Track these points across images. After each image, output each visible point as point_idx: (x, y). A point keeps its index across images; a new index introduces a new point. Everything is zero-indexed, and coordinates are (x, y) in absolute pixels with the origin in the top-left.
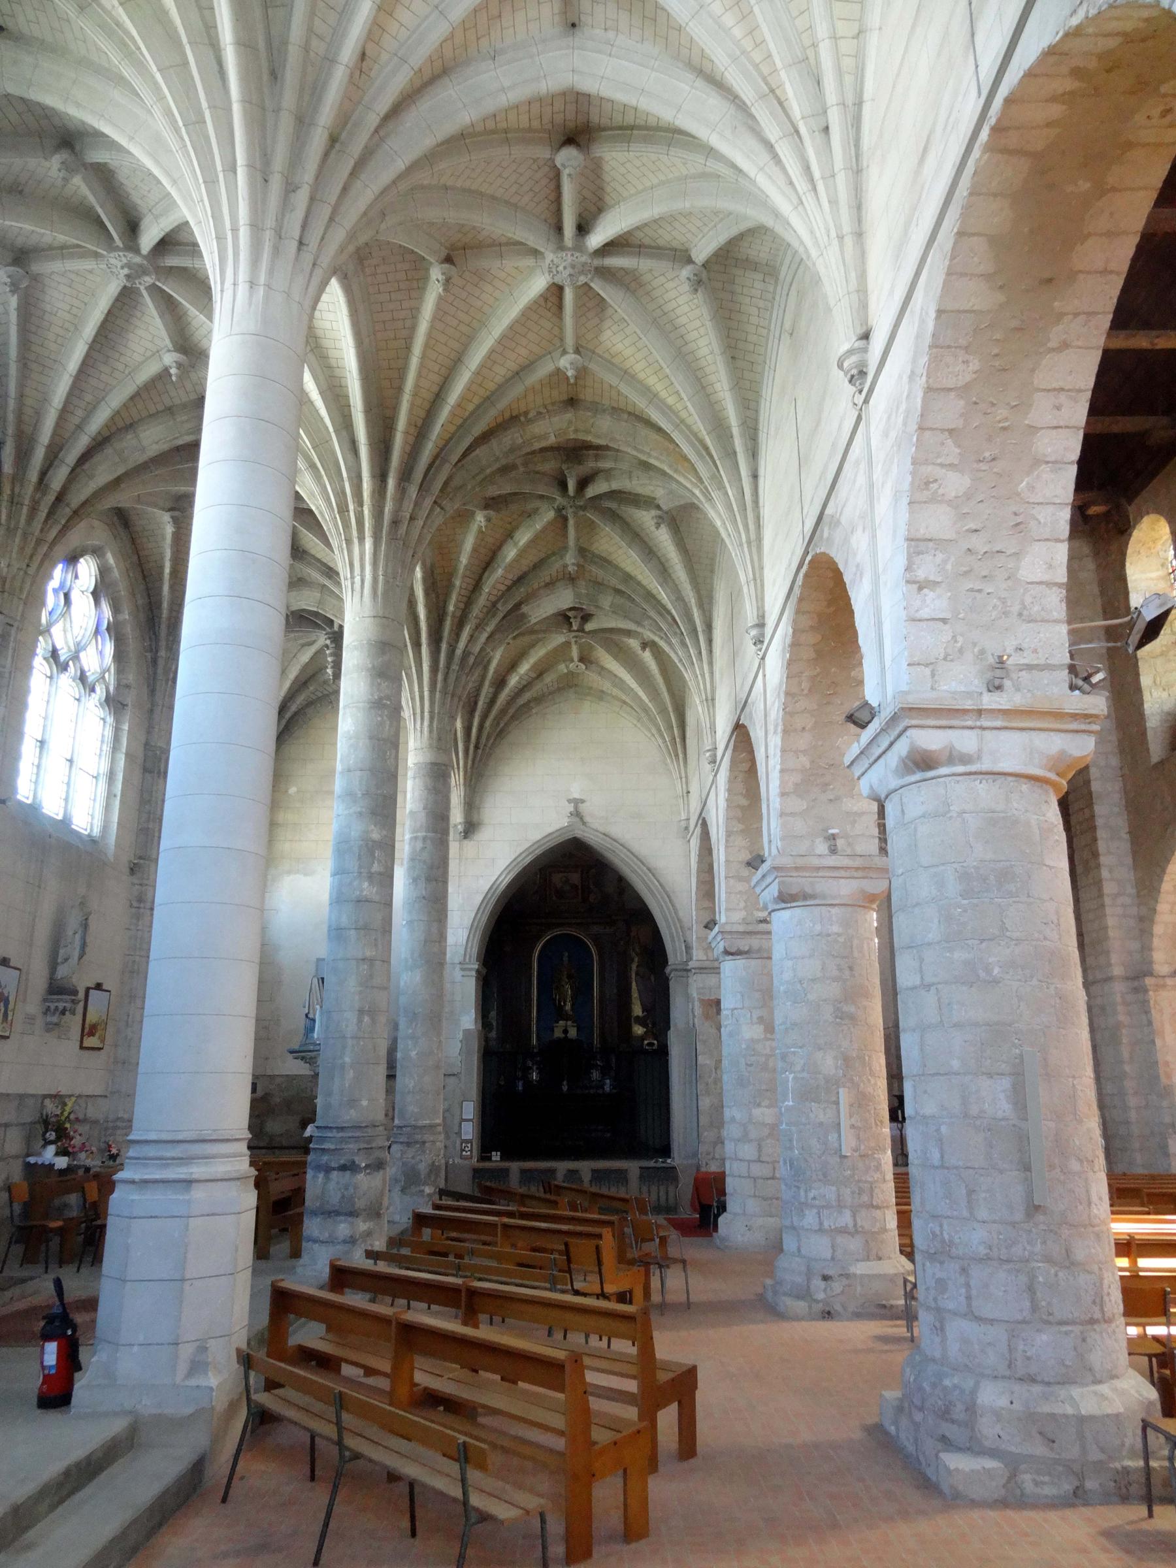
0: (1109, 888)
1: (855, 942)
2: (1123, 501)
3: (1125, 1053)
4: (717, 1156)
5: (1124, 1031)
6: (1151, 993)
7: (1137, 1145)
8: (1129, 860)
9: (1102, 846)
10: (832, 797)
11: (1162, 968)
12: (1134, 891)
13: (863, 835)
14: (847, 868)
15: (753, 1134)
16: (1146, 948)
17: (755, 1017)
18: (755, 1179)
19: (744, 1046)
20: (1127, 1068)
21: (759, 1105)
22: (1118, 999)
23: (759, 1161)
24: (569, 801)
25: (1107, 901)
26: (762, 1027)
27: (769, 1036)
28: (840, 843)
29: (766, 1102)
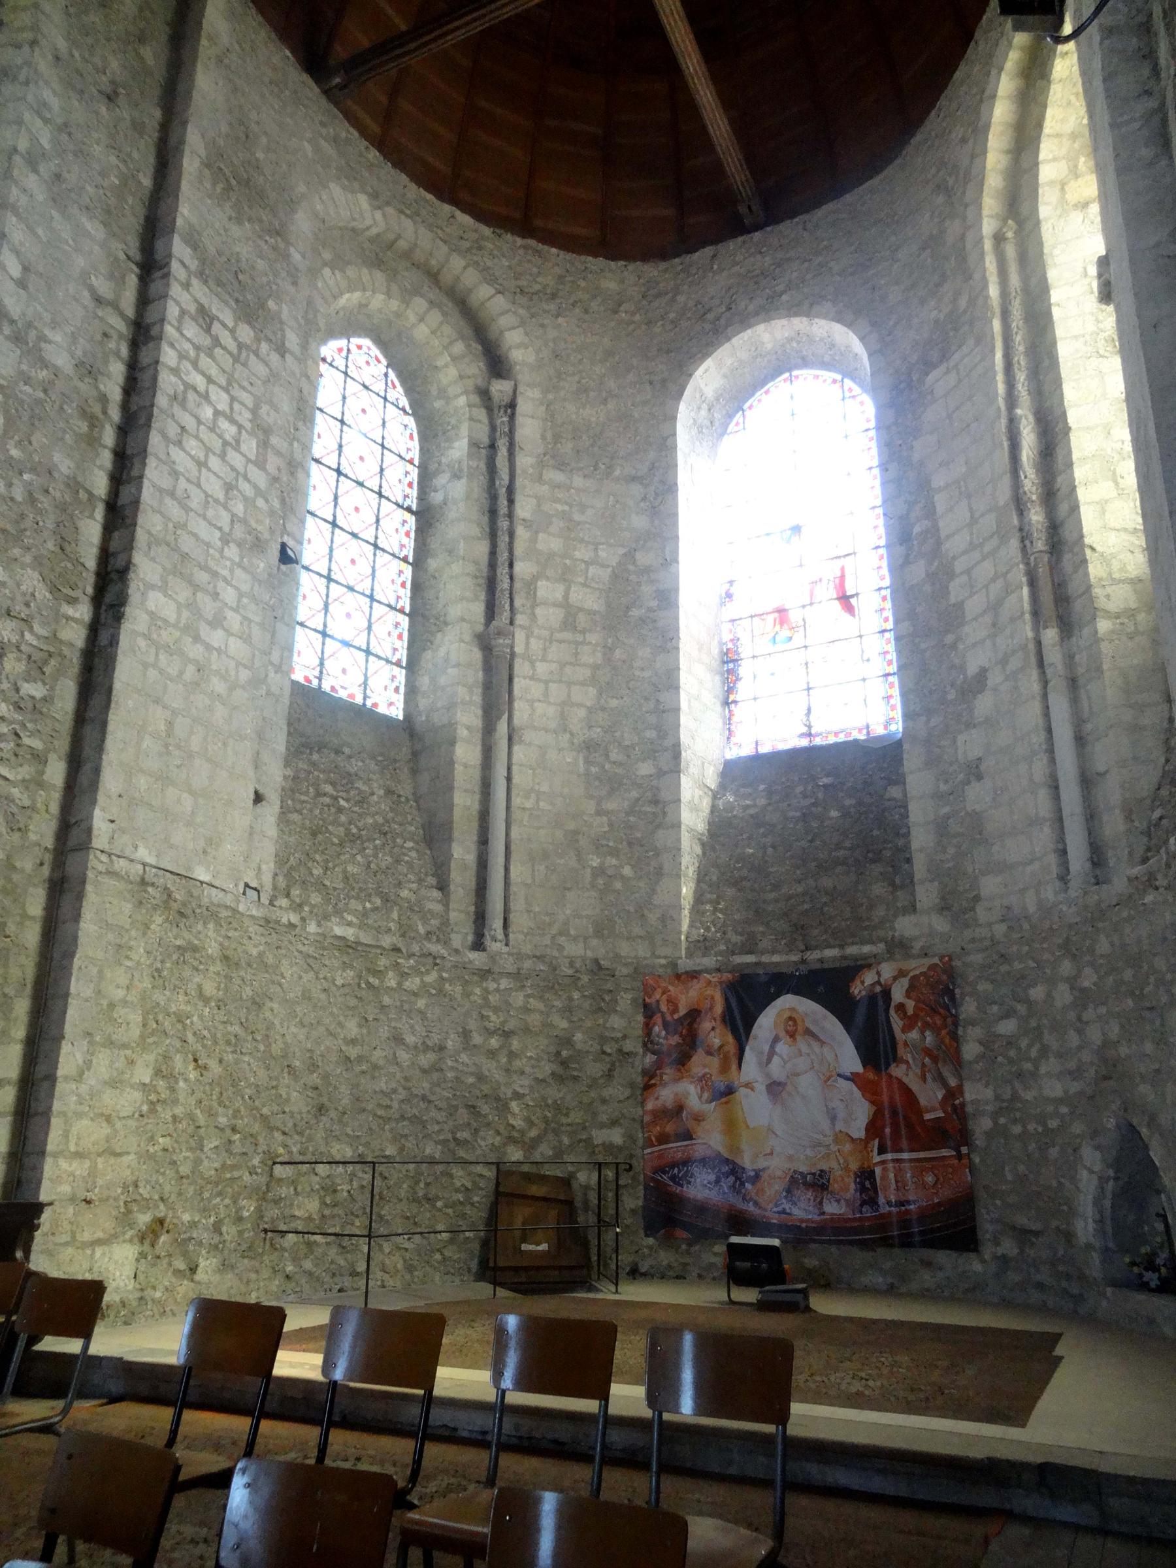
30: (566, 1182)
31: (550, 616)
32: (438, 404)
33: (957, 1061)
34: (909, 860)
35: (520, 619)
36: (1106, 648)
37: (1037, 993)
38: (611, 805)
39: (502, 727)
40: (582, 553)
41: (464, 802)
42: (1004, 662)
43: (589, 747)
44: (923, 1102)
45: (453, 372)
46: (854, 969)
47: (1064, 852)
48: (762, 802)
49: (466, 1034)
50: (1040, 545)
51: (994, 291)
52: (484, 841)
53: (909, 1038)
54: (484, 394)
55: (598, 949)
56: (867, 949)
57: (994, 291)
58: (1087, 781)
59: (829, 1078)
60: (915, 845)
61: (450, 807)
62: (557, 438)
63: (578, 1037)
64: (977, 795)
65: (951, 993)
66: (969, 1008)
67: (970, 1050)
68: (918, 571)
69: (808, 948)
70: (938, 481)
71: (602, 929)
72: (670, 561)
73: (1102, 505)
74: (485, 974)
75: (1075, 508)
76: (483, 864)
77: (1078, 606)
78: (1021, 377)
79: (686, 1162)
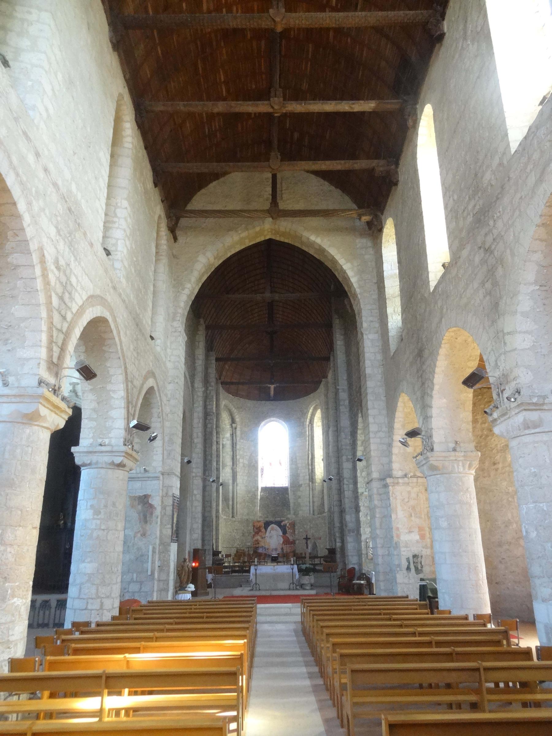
0: (373, 428)
1: (8, 448)
2: (379, 214)
3: (378, 524)
4: (130, 590)
5: (377, 510)
6: (390, 487)
7: (381, 578)
8: (384, 412)
9: (370, 404)
10: (10, 348)
11: (397, 472)
12: (387, 429)
13: (28, 373)
14: (8, 396)
15: (78, 581)
16: (390, 462)
17: (89, 504)
18: (75, 610)
19: (81, 524)
20: (378, 532)
21: (83, 562)
22: (375, 491)
23: (79, 598)
24: (70, 384)
25: (371, 435)
26: (92, 511)
27: (96, 517)
28: (11, 379)
29: (89, 560)
30: (244, 550)
31: (241, 465)
32: (224, 426)
33: (294, 534)
34: (290, 507)
35: (238, 466)
36: (317, 487)
37: (305, 526)
38: (249, 495)
39: (235, 484)
40: (245, 454)
41: (231, 495)
42: (305, 484)
43: (246, 486)
44: (290, 539)
45: (228, 422)
46: (282, 521)
47: (310, 511)
48: (268, 495)
49: (233, 530)
50: (310, 471)
51: (307, 433)
52: (233, 501)
53: (289, 531)
54: (231, 425)
55: (247, 517)
56: (284, 519)
57: (307, 433)
58: (313, 502)
59: (277, 536)
60: (291, 505)
61: (229, 496)
62: (242, 434)
63: (245, 530)
64: (300, 501)
65: (294, 525)
66: (296, 527)
67: (296, 533)
68: (294, 466)
69: (275, 518)
70: (297, 455)
71: (248, 514)
72: (257, 456)
73: (318, 469)
74: (235, 521)
75: (315, 468)
76: (233, 504)
77: (314, 480)
78: (310, 447)
79: (258, 547)
